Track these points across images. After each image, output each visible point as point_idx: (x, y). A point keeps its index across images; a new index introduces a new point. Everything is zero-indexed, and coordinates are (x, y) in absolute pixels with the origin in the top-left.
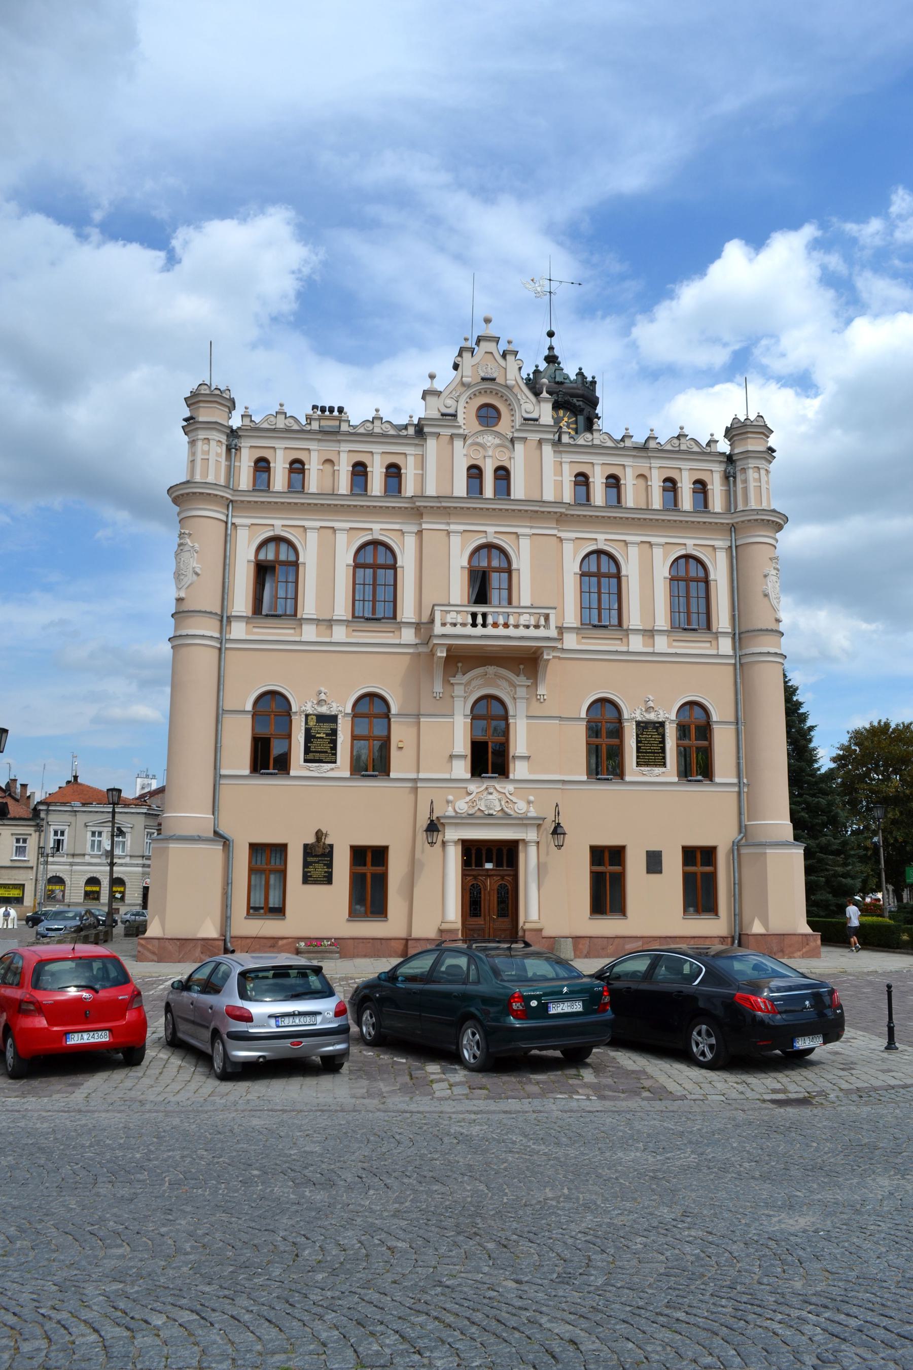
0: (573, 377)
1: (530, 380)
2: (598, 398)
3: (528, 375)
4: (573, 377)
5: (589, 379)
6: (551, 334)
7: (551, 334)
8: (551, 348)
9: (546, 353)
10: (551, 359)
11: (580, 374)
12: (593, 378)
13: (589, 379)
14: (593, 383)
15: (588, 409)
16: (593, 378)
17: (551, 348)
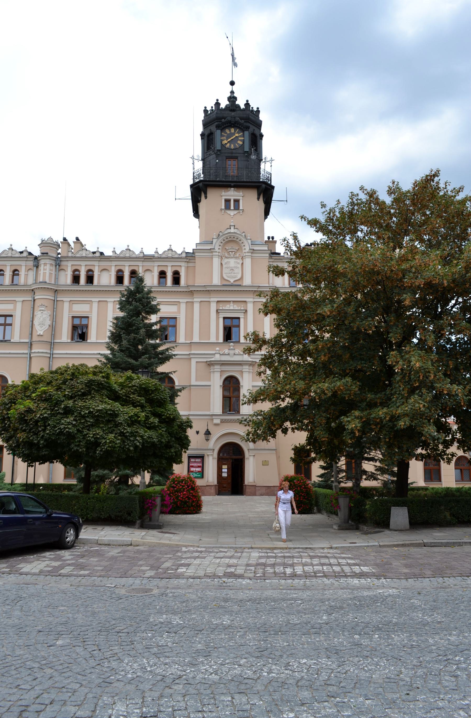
0: (242, 107)
1: (212, 110)
2: (261, 121)
3: (212, 107)
4: (242, 107)
5: (255, 109)
6: (232, 83)
7: (232, 83)
8: (232, 92)
9: (229, 95)
10: (232, 99)
11: (247, 105)
12: (258, 108)
13: (255, 109)
14: (258, 111)
15: (252, 128)
16: (258, 108)
17: (232, 92)
